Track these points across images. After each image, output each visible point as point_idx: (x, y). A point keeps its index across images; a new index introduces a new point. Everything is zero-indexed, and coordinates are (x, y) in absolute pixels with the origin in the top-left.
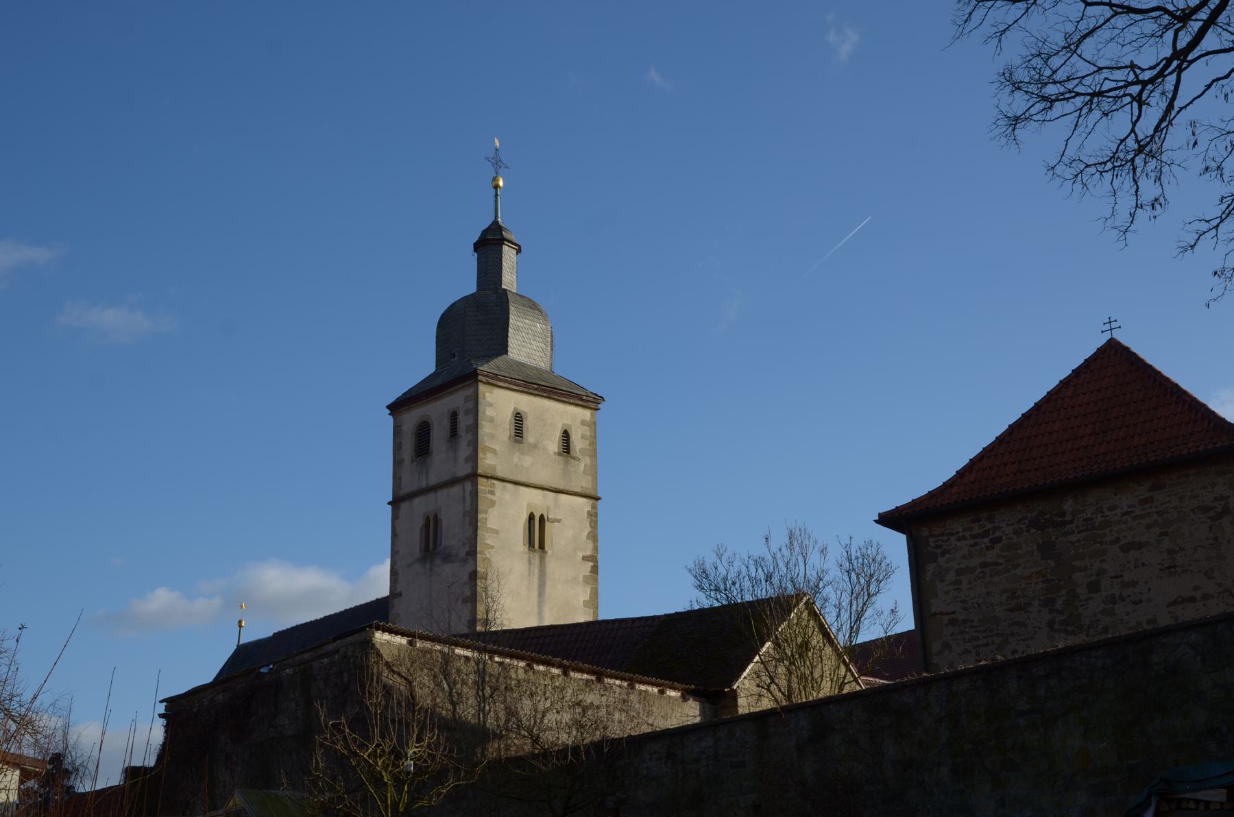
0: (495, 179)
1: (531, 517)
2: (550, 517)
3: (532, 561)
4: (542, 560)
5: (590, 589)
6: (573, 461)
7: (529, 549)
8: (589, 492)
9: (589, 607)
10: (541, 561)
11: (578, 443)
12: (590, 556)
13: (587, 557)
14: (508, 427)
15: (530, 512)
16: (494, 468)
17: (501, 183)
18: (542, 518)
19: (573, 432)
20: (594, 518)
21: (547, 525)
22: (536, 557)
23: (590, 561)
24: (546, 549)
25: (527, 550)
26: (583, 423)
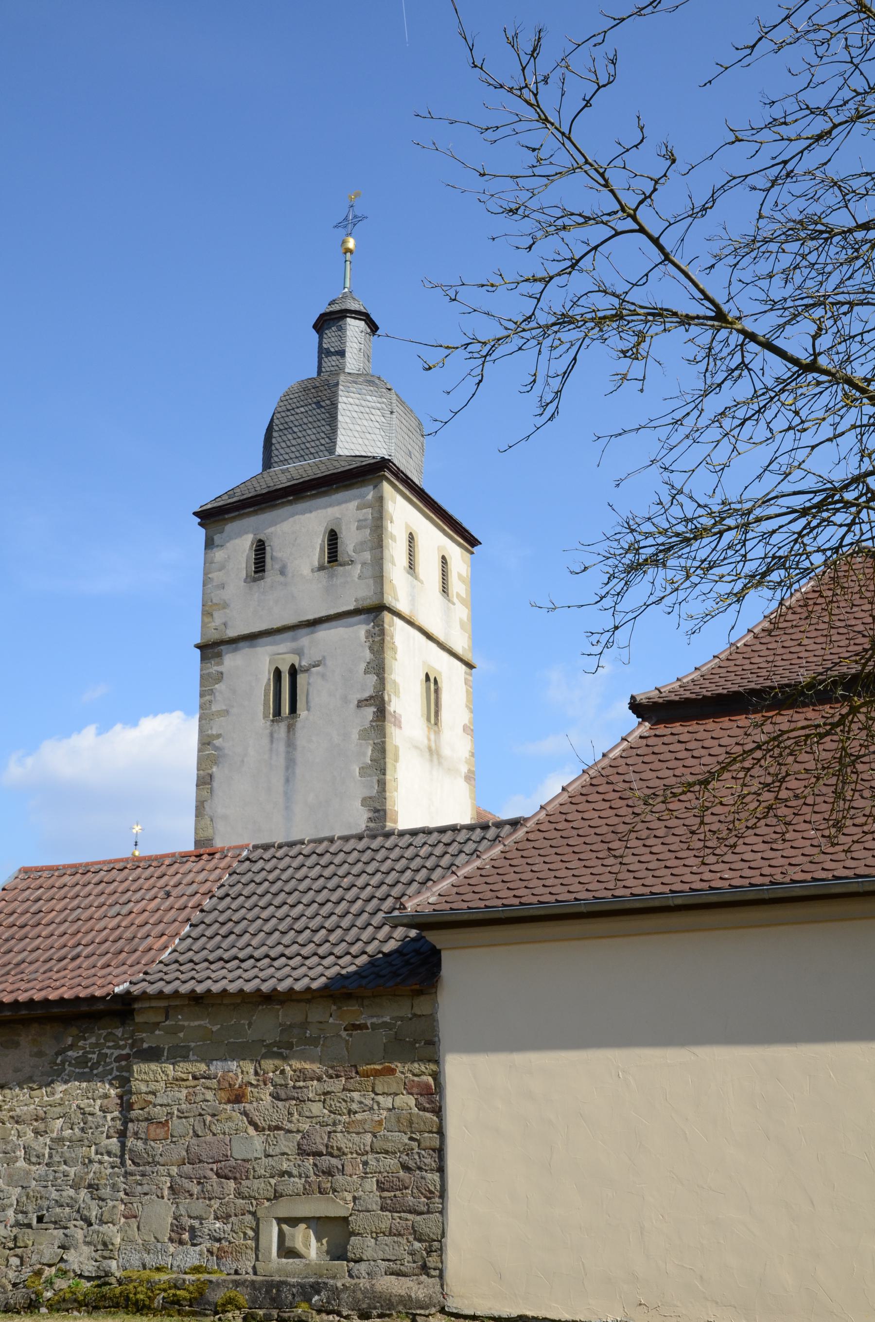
0: (344, 242)
1: (278, 673)
2: (304, 663)
3: (275, 735)
4: (291, 728)
5: (370, 748)
6: (341, 568)
7: (273, 721)
8: (368, 603)
9: (370, 776)
10: (289, 731)
11: (349, 541)
12: (371, 697)
13: (367, 700)
14: (244, 565)
17: (351, 243)
18: (294, 672)
19: (344, 527)
20: (377, 639)
21: (301, 679)
22: (282, 728)
23: (371, 705)
24: (298, 712)
25: (269, 723)
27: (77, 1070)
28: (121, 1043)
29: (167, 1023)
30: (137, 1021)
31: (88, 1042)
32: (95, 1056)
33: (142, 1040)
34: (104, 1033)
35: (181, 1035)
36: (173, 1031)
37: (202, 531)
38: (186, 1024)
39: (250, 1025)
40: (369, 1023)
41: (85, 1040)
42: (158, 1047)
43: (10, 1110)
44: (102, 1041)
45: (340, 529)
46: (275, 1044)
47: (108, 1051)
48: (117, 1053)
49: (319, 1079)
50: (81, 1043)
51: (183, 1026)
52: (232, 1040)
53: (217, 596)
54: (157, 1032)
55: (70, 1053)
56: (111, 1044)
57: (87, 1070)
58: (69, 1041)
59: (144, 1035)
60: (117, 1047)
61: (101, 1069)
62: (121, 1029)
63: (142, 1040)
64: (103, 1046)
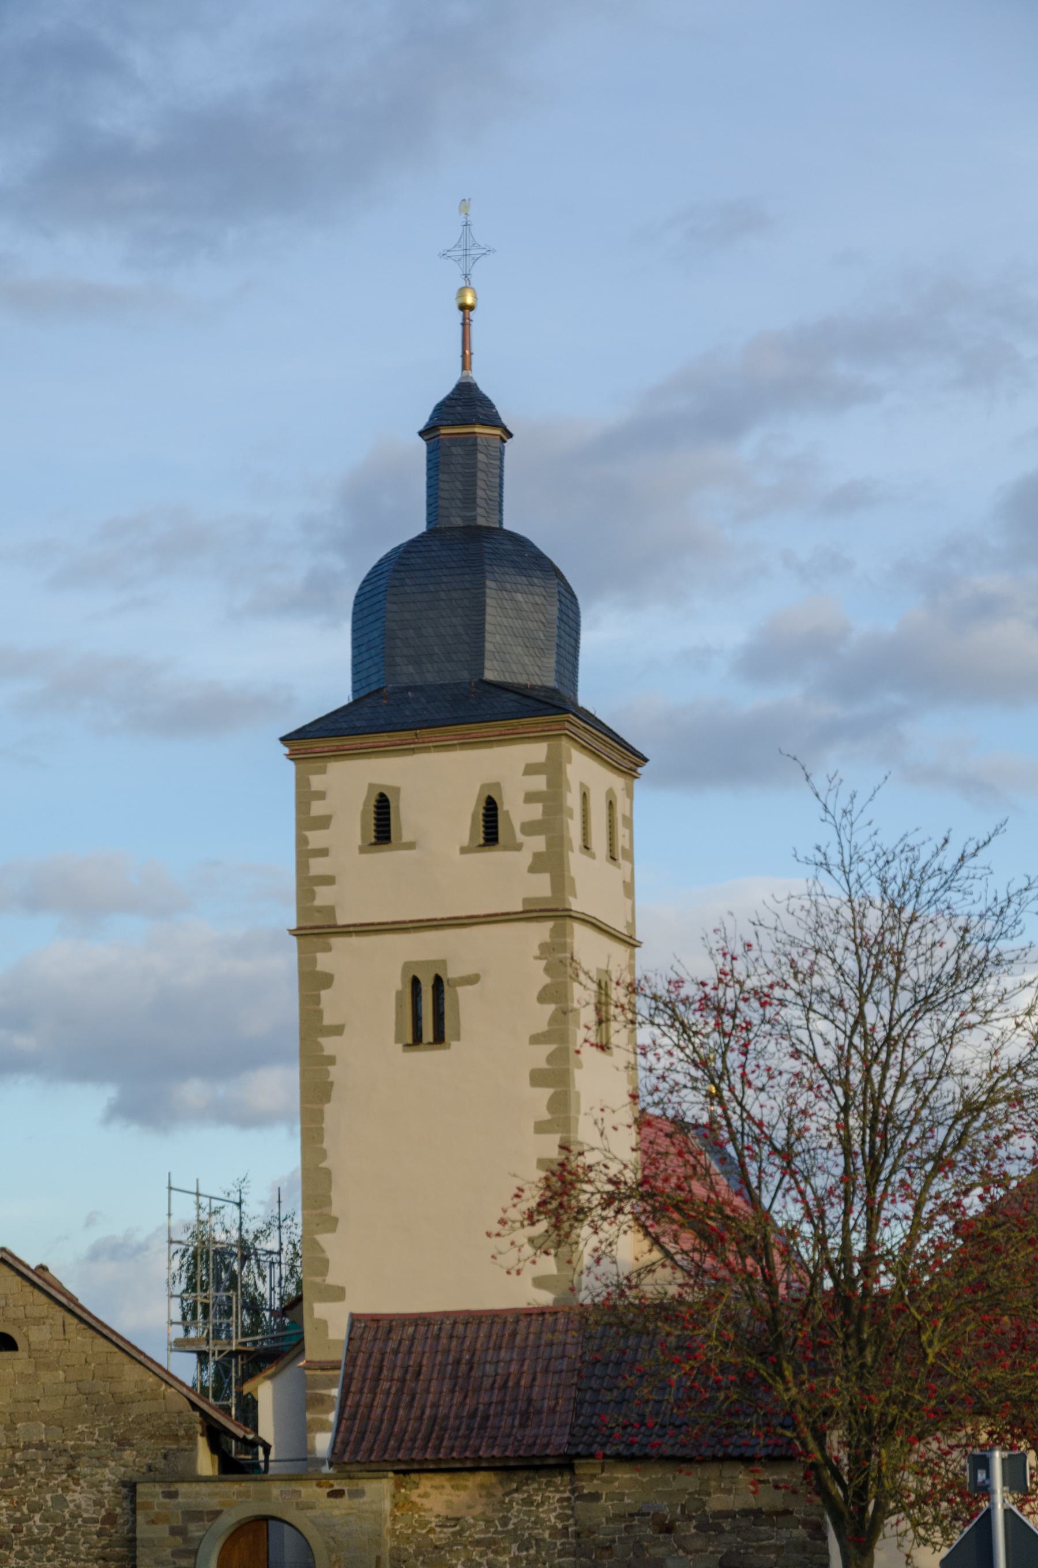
1: (416, 982)
15: (410, 976)
16: (330, 911)
18: (438, 983)
26: (531, 770)
27: (525, 1508)
28: (562, 1489)
29: (604, 1475)
30: (577, 1472)
31: (531, 1487)
32: (539, 1498)
33: (583, 1487)
34: (544, 1480)
35: (616, 1484)
36: (608, 1481)
37: (291, 766)
38: (620, 1476)
39: (674, 1478)
40: (771, 1479)
41: (528, 1485)
42: (597, 1493)
43: (471, 1536)
44: (544, 1486)
45: (501, 798)
46: (696, 1492)
47: (551, 1495)
48: (558, 1496)
49: (734, 1517)
50: (525, 1488)
51: (617, 1479)
52: (660, 1489)
53: (318, 866)
54: (595, 1482)
55: (516, 1495)
56: (552, 1489)
57: (533, 1508)
58: (514, 1485)
59: (584, 1483)
60: (557, 1491)
61: (546, 1508)
62: (559, 1478)
63: (583, 1487)
64: (545, 1490)
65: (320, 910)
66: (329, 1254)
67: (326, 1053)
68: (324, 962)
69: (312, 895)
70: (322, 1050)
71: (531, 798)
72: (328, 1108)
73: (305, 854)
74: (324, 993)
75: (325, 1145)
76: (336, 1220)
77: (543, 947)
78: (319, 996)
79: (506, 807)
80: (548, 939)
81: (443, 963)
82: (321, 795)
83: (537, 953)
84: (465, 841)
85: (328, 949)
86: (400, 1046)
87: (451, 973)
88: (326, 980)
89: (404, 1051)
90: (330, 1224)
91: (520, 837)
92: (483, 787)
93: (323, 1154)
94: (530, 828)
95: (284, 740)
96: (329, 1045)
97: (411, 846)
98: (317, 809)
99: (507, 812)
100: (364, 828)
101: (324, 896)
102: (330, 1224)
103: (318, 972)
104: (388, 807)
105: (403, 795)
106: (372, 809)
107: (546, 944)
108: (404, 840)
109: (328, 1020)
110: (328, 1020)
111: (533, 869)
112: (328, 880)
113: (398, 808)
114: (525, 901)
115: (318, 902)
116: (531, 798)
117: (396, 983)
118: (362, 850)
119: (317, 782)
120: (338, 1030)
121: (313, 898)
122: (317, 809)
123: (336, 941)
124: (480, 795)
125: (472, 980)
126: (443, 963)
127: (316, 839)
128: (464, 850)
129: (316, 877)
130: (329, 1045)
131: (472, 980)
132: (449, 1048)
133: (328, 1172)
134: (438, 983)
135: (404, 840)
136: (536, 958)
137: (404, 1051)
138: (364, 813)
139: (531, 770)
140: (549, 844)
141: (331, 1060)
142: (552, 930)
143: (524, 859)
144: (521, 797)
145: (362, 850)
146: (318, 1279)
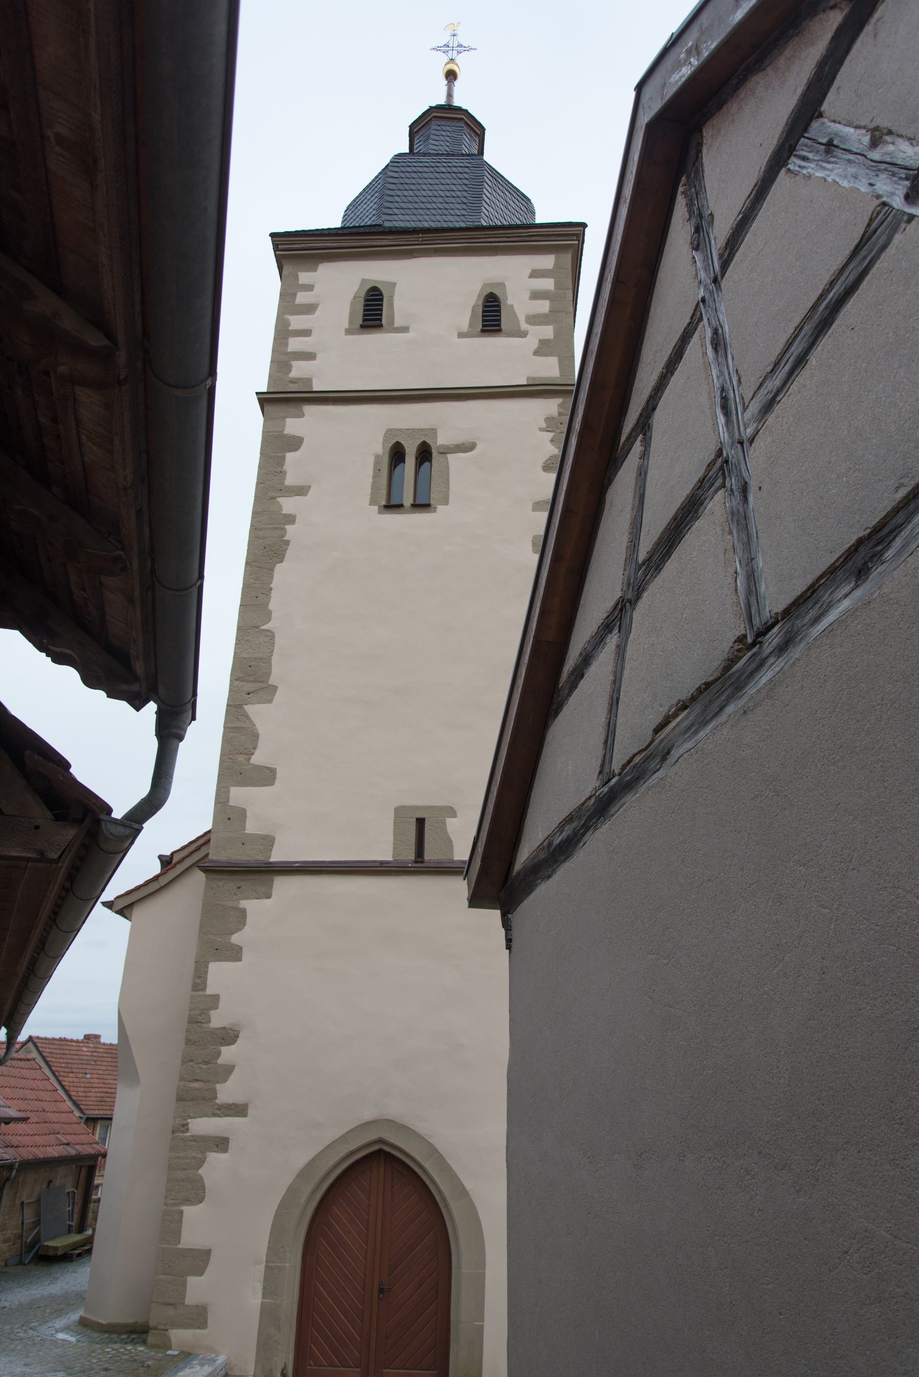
65: (293, 381)
66: (261, 729)
67: (284, 511)
68: (293, 426)
69: (289, 368)
70: (282, 509)
71: (536, 295)
72: (279, 568)
73: (283, 333)
74: (290, 456)
75: (271, 607)
76: (275, 688)
77: (548, 420)
78: (283, 458)
79: (509, 302)
80: (556, 414)
81: (433, 431)
82: (309, 288)
83: (544, 425)
84: (465, 326)
85: (302, 415)
86: (376, 508)
87: (443, 439)
88: (295, 443)
89: (380, 512)
90: (267, 692)
91: (524, 326)
92: (485, 285)
93: (268, 616)
94: (534, 320)
95: (273, 235)
96: (288, 505)
97: (405, 329)
98: (302, 298)
99: (512, 306)
100: (352, 315)
101: (299, 369)
102: (267, 692)
103: (286, 436)
104: (382, 300)
105: (397, 289)
106: (361, 302)
107: (553, 418)
108: (396, 325)
109: (290, 480)
110: (290, 480)
111: (537, 353)
112: (309, 356)
113: (391, 298)
114: (528, 379)
115: (294, 374)
116: (536, 295)
117: (379, 448)
118: (349, 332)
119: (304, 277)
120: (301, 491)
121: (290, 371)
122: (302, 298)
123: (309, 409)
124: (481, 291)
125: (467, 447)
126: (433, 431)
127: (297, 322)
128: (461, 335)
129: (294, 353)
130: (288, 505)
131: (467, 447)
132: (435, 511)
133: (271, 635)
134: (425, 454)
135: (396, 325)
136: (541, 430)
137: (380, 512)
138: (353, 304)
139: (536, 274)
140: (557, 334)
141: (291, 519)
142: (560, 406)
143: (531, 342)
144: (527, 295)
145: (349, 332)
146: (241, 758)
